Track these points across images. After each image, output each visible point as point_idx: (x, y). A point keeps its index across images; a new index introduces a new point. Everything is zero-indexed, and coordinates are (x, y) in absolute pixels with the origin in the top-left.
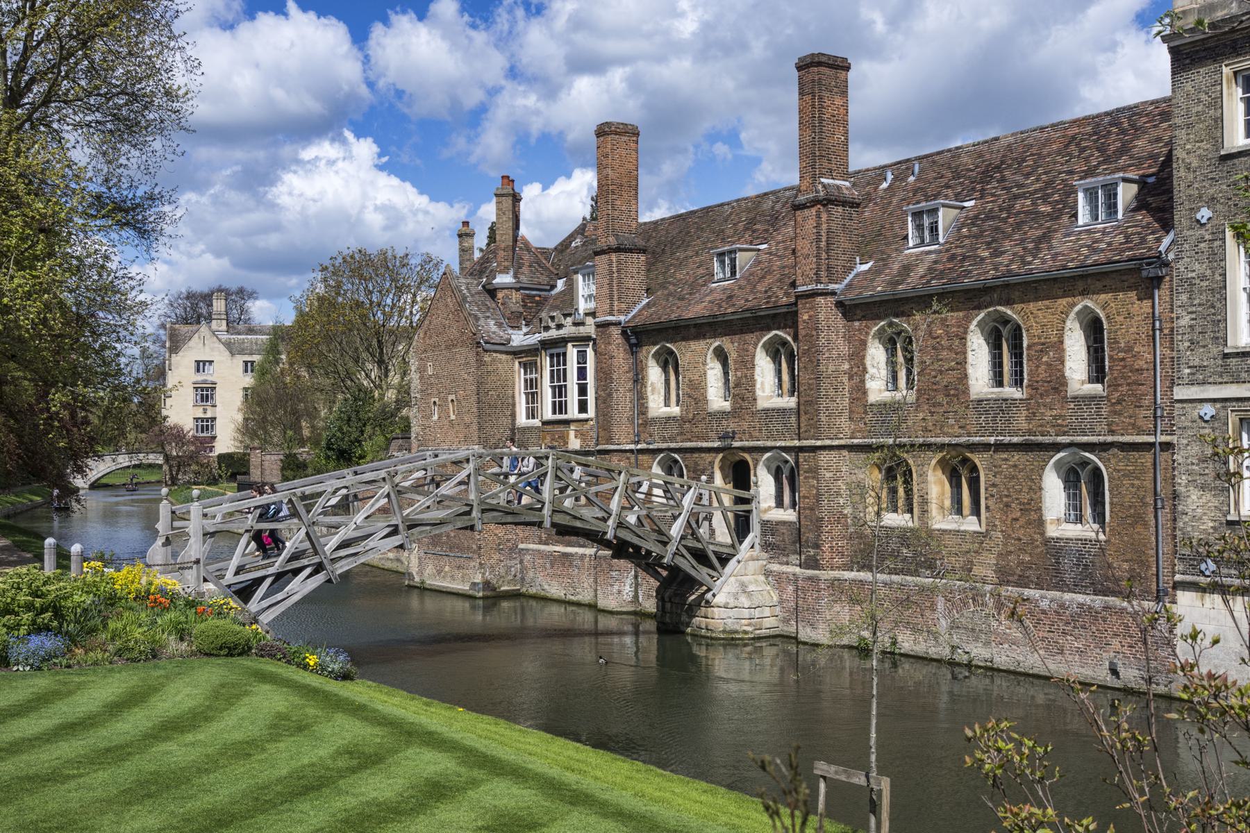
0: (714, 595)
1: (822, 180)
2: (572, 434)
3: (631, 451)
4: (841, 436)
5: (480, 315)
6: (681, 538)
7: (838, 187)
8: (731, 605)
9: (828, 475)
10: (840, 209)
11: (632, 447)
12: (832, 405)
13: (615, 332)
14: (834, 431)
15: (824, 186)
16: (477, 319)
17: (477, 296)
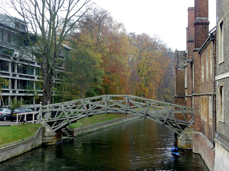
0: (179, 136)
1: (196, 18)
2: (186, 91)
3: (191, 96)
4: (199, 92)
5: (180, 61)
6: (168, 119)
7: (202, 19)
8: (182, 140)
9: (197, 104)
10: (201, 26)
11: (191, 95)
12: (198, 83)
13: (189, 64)
14: (198, 91)
15: (197, 19)
16: (179, 62)
17: (182, 56)
